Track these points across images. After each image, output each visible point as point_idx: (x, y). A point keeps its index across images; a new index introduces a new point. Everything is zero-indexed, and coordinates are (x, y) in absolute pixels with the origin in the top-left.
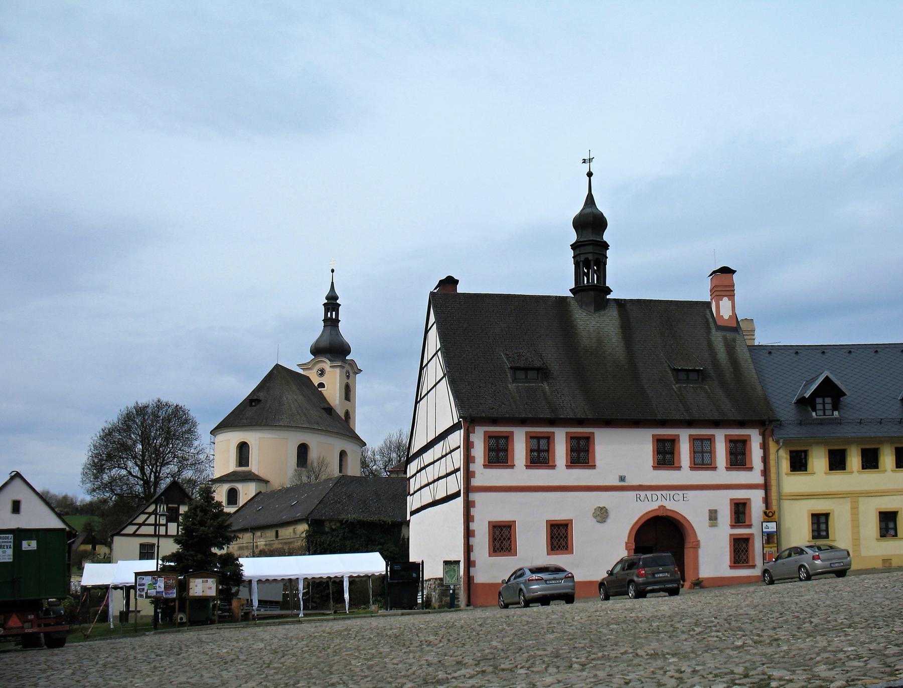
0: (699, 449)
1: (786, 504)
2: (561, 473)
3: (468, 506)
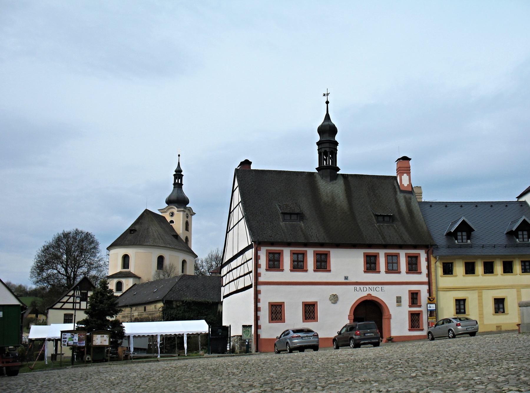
0: (391, 261)
1: (441, 294)
3: (257, 293)
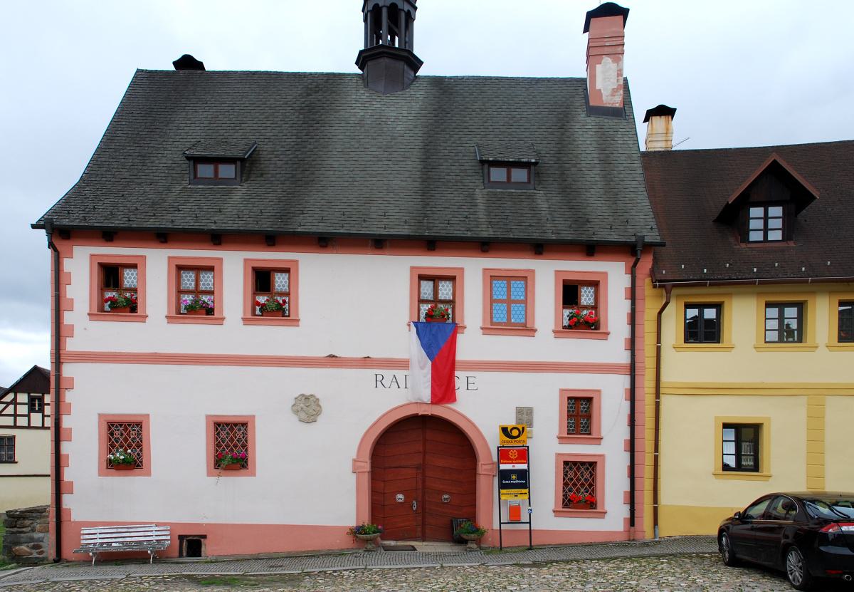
2: (234, 330)
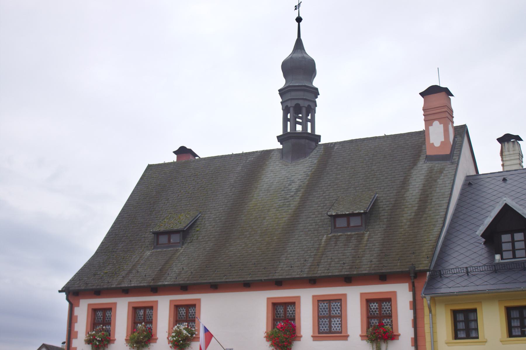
0: (326, 313)
